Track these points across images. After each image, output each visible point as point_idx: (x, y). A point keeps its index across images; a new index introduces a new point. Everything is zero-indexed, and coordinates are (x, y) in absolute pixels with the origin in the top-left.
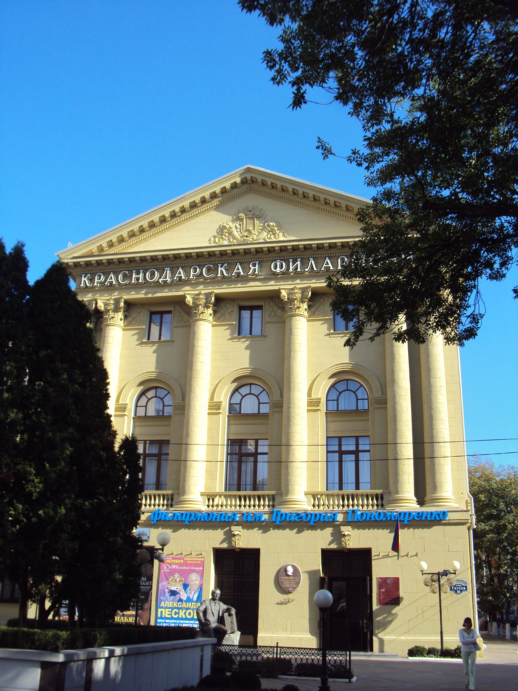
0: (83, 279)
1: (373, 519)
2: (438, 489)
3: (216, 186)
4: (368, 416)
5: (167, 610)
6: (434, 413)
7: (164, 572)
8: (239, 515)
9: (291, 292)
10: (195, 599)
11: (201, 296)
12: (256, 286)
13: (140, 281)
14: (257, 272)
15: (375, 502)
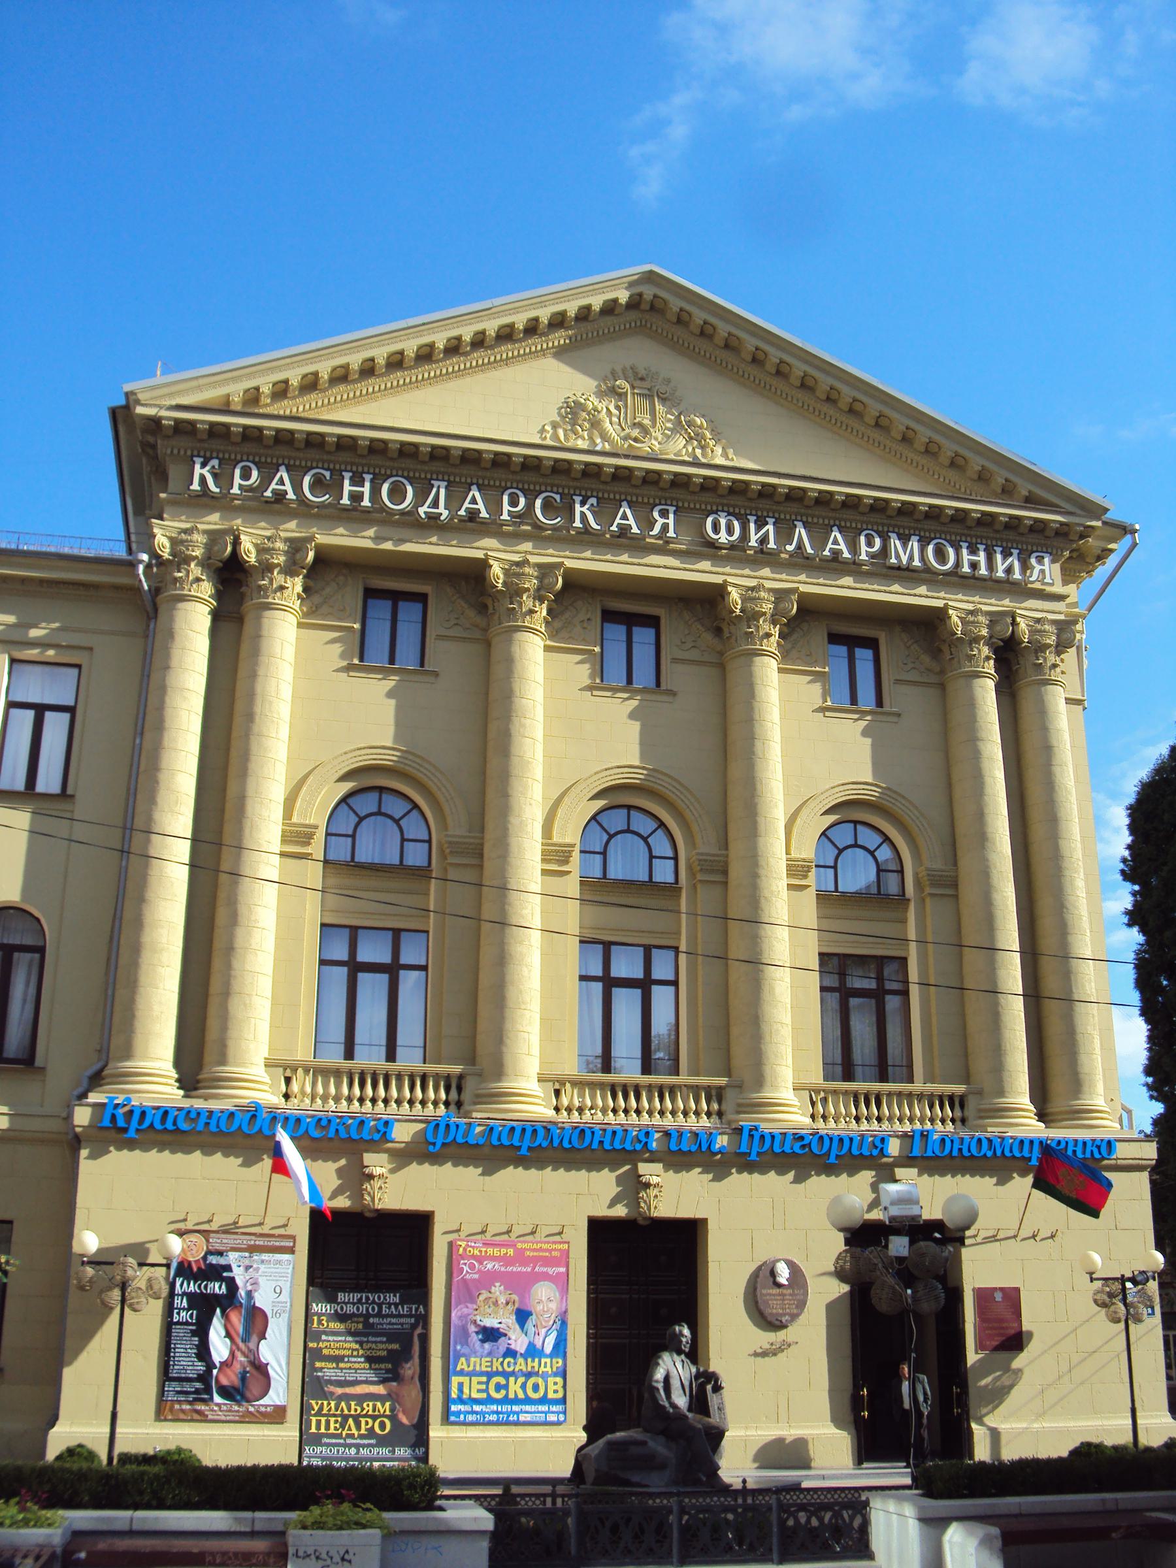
0: (198, 470)
2: (1085, 1088)
3: (567, 299)
4: (906, 909)
5: (475, 1379)
6: (1068, 917)
7: (464, 1280)
8: (657, 1135)
9: (749, 596)
10: (548, 1349)
11: (527, 570)
12: (665, 567)
13: (366, 502)
14: (671, 534)
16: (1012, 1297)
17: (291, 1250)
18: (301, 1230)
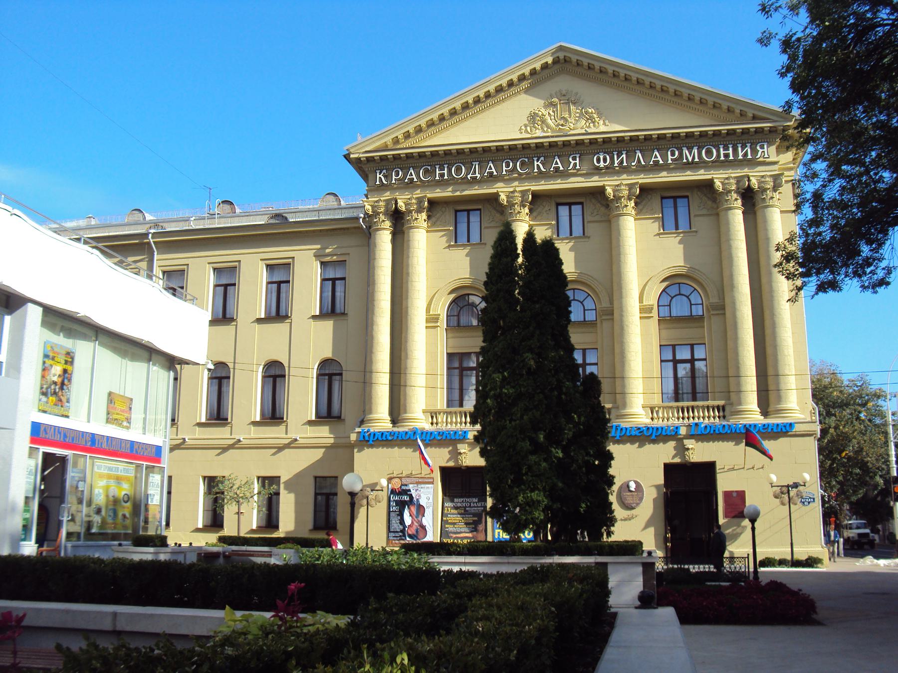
1: (717, 432)
2: (783, 399)
9: (616, 189)
11: (516, 194)
13: (446, 177)
14: (578, 167)
16: (741, 495)
17: (432, 483)
18: (437, 475)
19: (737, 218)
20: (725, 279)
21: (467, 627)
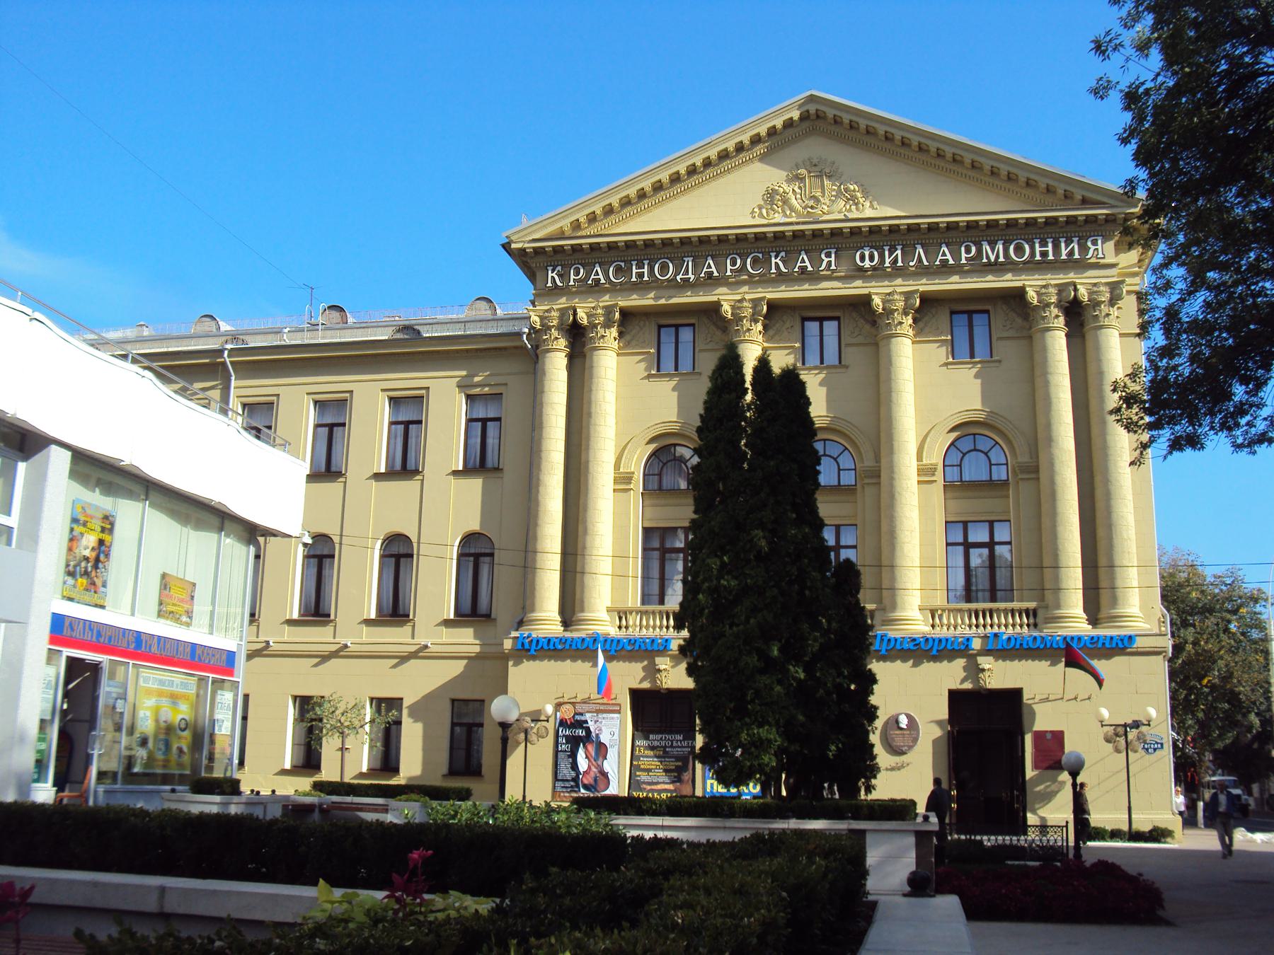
2: (1120, 602)
6: (1112, 488)
11: (745, 304)
13: (646, 278)
14: (833, 267)
15: (1025, 620)
16: (1058, 737)
17: (618, 712)
19: (1058, 343)
20: (1040, 429)
21: (661, 918)
